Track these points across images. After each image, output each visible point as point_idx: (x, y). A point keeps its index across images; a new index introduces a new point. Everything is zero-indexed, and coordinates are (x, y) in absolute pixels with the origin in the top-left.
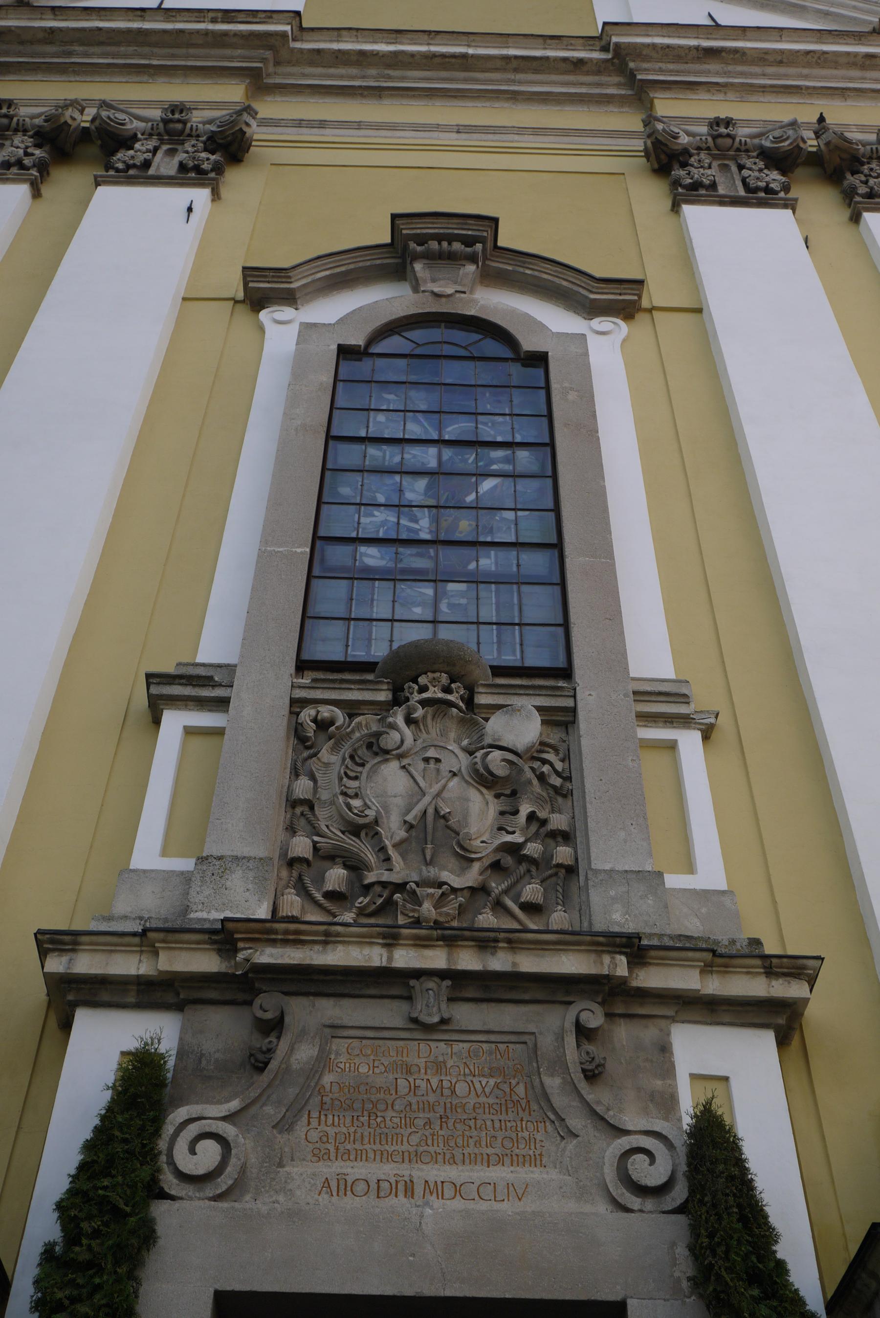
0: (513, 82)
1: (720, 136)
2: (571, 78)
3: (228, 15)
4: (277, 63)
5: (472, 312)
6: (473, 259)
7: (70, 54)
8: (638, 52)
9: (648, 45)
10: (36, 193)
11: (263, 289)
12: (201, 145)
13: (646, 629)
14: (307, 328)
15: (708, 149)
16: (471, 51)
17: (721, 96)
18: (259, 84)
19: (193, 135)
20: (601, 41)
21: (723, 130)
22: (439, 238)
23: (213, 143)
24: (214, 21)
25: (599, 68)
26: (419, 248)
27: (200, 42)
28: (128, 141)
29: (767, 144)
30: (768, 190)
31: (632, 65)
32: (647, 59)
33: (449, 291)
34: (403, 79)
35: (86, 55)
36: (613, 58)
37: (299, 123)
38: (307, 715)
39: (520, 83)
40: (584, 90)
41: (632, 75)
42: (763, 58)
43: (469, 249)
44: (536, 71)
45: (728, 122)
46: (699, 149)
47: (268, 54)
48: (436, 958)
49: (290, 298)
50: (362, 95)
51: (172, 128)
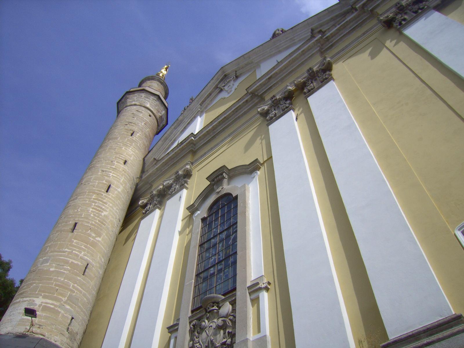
0: (237, 115)
1: (273, 101)
2: (247, 105)
4: (195, 145)
5: (224, 193)
7: (162, 170)
8: (256, 90)
9: (256, 87)
12: (182, 178)
15: (273, 105)
16: (225, 115)
17: (278, 85)
22: (216, 177)
24: (180, 146)
25: (252, 98)
26: (213, 182)
27: (180, 152)
30: (287, 108)
31: (256, 93)
32: (258, 90)
36: (252, 95)
38: (192, 324)
39: (239, 114)
40: (251, 106)
42: (281, 70)
43: (222, 176)
44: (240, 109)
45: (274, 96)
46: (271, 107)
47: (192, 145)
50: (212, 140)
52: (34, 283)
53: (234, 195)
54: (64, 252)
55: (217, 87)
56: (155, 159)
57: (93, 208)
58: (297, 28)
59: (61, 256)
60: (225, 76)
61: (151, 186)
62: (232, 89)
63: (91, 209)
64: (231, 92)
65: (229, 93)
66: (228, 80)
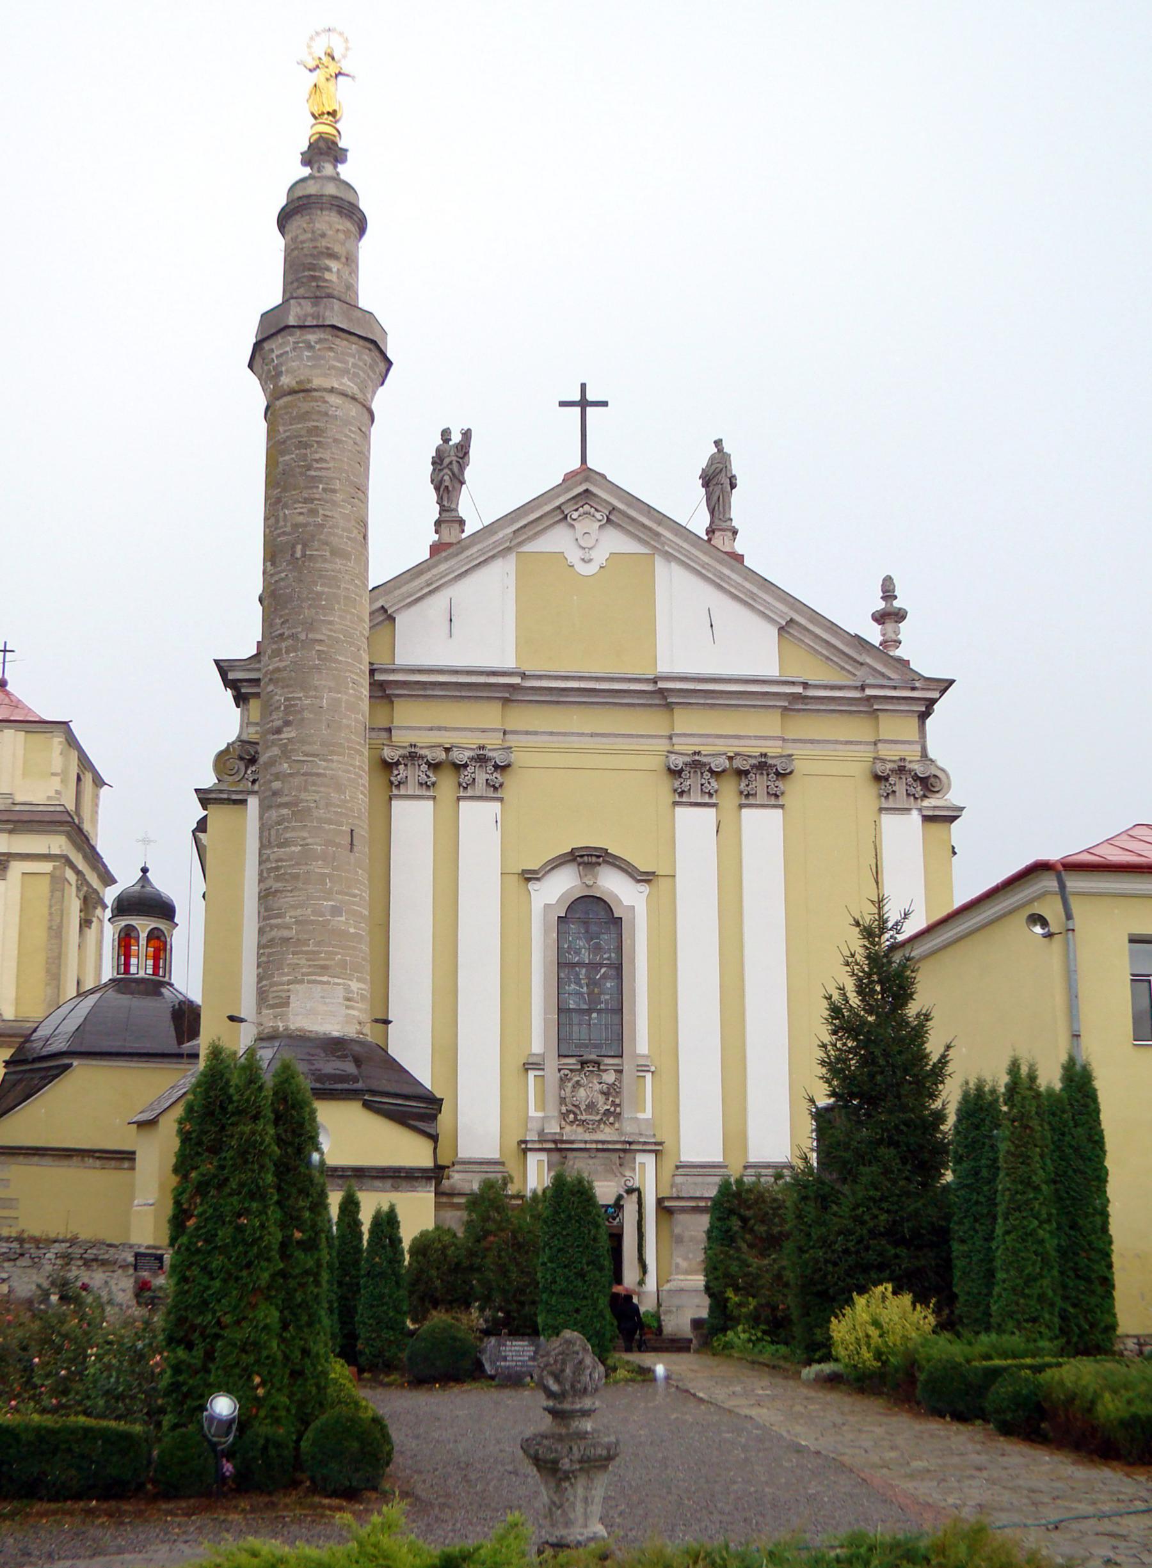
3: (494, 673)
6: (599, 864)
7: (425, 689)
10: (434, 798)
11: (529, 877)
13: (642, 1046)
14: (547, 906)
18: (506, 701)
19: (489, 759)
20: (655, 681)
21: (697, 758)
23: (496, 767)
28: (465, 766)
29: (713, 766)
33: (591, 883)
34: (567, 696)
35: (433, 689)
37: (527, 733)
41: (665, 698)
45: (699, 753)
48: (594, 1146)
49: (538, 879)
51: (481, 759)
52: (339, 953)
53: (616, 915)
54: (355, 896)
55: (559, 507)
56: (383, 607)
57: (362, 793)
58: (773, 588)
59: (354, 903)
60: (587, 491)
61: (389, 699)
62: (593, 554)
63: (361, 796)
64: (590, 560)
65: (583, 560)
66: (587, 507)
